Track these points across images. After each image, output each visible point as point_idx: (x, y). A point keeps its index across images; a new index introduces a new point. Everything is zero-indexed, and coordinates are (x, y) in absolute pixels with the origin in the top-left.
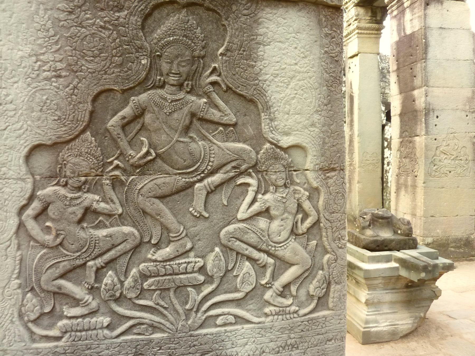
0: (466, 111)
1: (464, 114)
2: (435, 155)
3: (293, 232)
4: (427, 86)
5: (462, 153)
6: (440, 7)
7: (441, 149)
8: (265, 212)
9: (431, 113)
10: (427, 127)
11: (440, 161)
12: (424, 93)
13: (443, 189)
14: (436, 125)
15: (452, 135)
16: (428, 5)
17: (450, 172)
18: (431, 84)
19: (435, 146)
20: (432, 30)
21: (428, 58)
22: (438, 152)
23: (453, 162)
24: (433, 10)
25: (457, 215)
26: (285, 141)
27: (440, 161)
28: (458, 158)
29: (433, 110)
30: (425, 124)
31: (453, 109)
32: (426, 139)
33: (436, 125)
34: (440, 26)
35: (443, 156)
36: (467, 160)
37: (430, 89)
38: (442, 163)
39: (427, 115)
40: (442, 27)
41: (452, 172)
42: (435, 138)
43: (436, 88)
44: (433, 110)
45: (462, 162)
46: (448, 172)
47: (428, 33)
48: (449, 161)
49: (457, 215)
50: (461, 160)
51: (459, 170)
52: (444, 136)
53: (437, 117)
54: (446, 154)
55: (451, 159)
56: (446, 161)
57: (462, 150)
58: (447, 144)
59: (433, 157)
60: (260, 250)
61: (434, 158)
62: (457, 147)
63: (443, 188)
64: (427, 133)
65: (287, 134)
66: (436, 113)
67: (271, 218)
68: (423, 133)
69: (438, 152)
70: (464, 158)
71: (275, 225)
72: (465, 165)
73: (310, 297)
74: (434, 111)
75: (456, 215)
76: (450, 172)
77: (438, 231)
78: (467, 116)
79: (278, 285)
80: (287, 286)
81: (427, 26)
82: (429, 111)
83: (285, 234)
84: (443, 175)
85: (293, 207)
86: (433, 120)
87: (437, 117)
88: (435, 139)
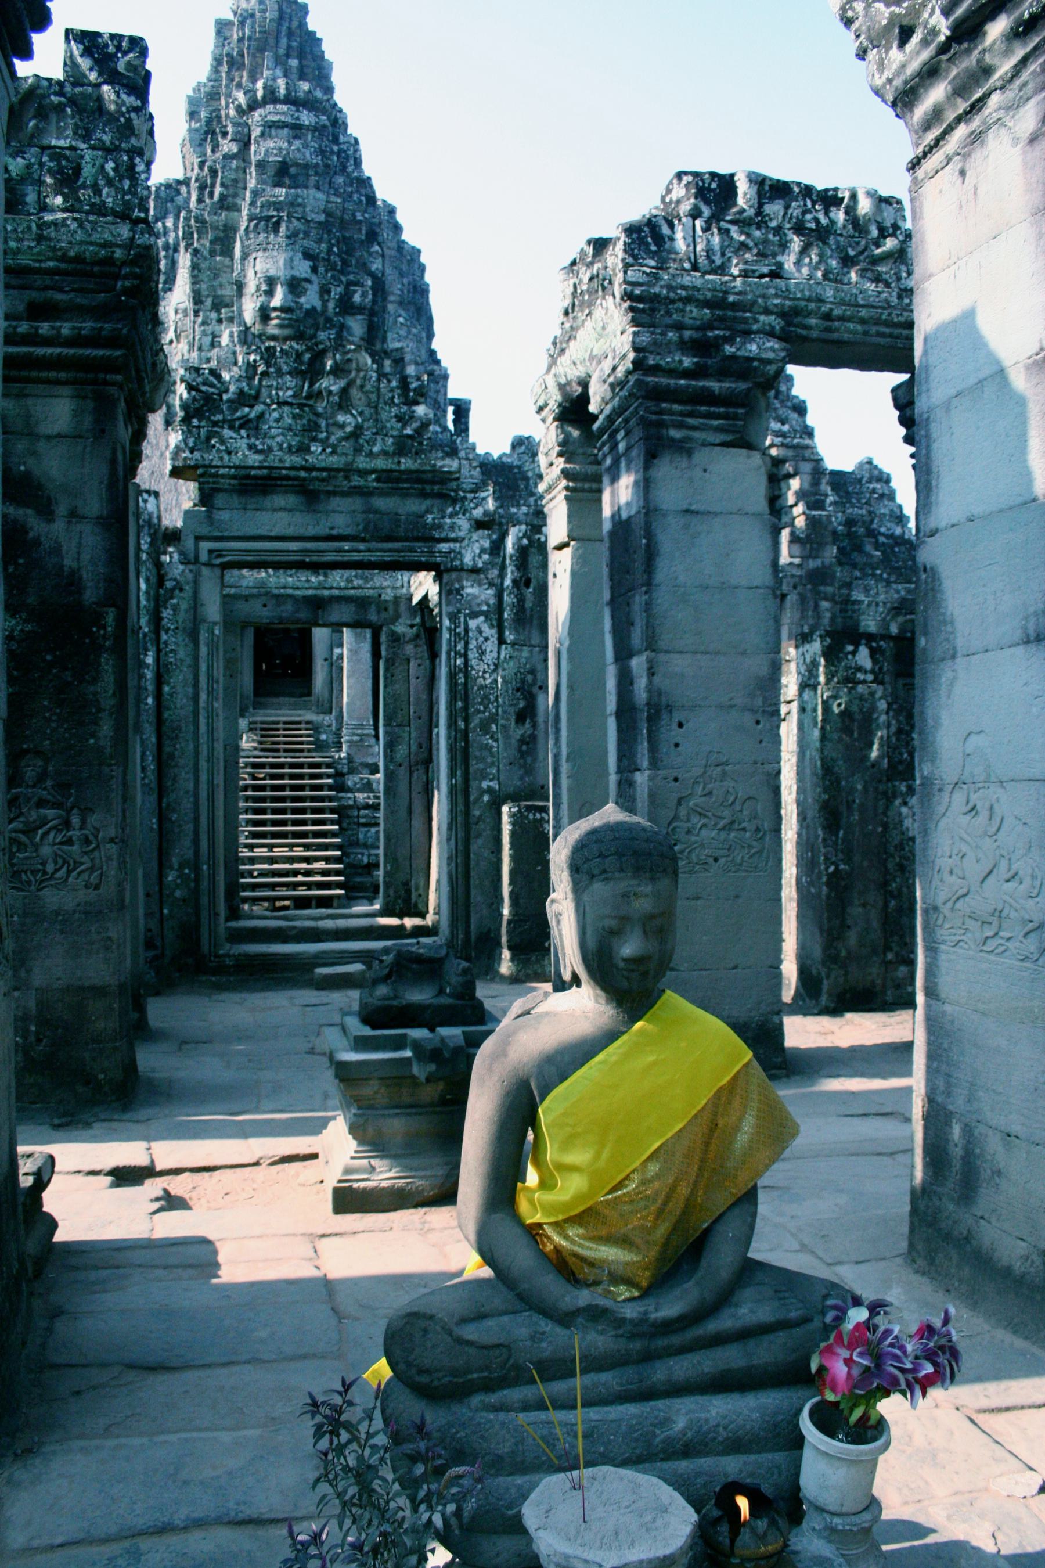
0: (753, 711)
1: (748, 719)
2: (676, 818)
4: (653, 651)
5: (745, 813)
6: (684, 464)
7: (691, 804)
9: (665, 716)
10: (653, 749)
11: (688, 832)
12: (645, 666)
13: (699, 902)
14: (677, 745)
15: (719, 769)
16: (654, 457)
17: (716, 860)
18: (662, 644)
19: (674, 797)
20: (665, 515)
21: (656, 582)
22: (683, 812)
23: (723, 835)
24: (665, 469)
25: (735, 967)
27: (688, 832)
28: (736, 826)
29: (670, 709)
30: (649, 742)
31: (721, 707)
32: (651, 778)
33: (677, 745)
34: (685, 507)
35: (695, 819)
36: (757, 830)
37: (662, 657)
38: (693, 839)
39: (653, 718)
40: (693, 508)
41: (722, 861)
42: (675, 774)
43: (677, 656)
44: (670, 709)
45: (748, 834)
46: (711, 860)
47: (654, 524)
48: (714, 833)
49: (735, 967)
51: (739, 855)
52: (697, 771)
53: (680, 725)
54: (705, 816)
55: (720, 826)
56: (704, 832)
57: (746, 806)
58: (706, 791)
59: (670, 824)
61: (674, 824)
62: (731, 799)
63: (698, 898)
64: (654, 764)
66: (677, 716)
68: (645, 763)
69: (683, 812)
70: (750, 826)
72: (755, 843)
74: (671, 711)
75: (732, 965)
76: (716, 860)
78: (758, 722)
81: (652, 506)
82: (658, 712)
84: (697, 868)
86: (669, 733)
87: (680, 725)
88: (676, 780)
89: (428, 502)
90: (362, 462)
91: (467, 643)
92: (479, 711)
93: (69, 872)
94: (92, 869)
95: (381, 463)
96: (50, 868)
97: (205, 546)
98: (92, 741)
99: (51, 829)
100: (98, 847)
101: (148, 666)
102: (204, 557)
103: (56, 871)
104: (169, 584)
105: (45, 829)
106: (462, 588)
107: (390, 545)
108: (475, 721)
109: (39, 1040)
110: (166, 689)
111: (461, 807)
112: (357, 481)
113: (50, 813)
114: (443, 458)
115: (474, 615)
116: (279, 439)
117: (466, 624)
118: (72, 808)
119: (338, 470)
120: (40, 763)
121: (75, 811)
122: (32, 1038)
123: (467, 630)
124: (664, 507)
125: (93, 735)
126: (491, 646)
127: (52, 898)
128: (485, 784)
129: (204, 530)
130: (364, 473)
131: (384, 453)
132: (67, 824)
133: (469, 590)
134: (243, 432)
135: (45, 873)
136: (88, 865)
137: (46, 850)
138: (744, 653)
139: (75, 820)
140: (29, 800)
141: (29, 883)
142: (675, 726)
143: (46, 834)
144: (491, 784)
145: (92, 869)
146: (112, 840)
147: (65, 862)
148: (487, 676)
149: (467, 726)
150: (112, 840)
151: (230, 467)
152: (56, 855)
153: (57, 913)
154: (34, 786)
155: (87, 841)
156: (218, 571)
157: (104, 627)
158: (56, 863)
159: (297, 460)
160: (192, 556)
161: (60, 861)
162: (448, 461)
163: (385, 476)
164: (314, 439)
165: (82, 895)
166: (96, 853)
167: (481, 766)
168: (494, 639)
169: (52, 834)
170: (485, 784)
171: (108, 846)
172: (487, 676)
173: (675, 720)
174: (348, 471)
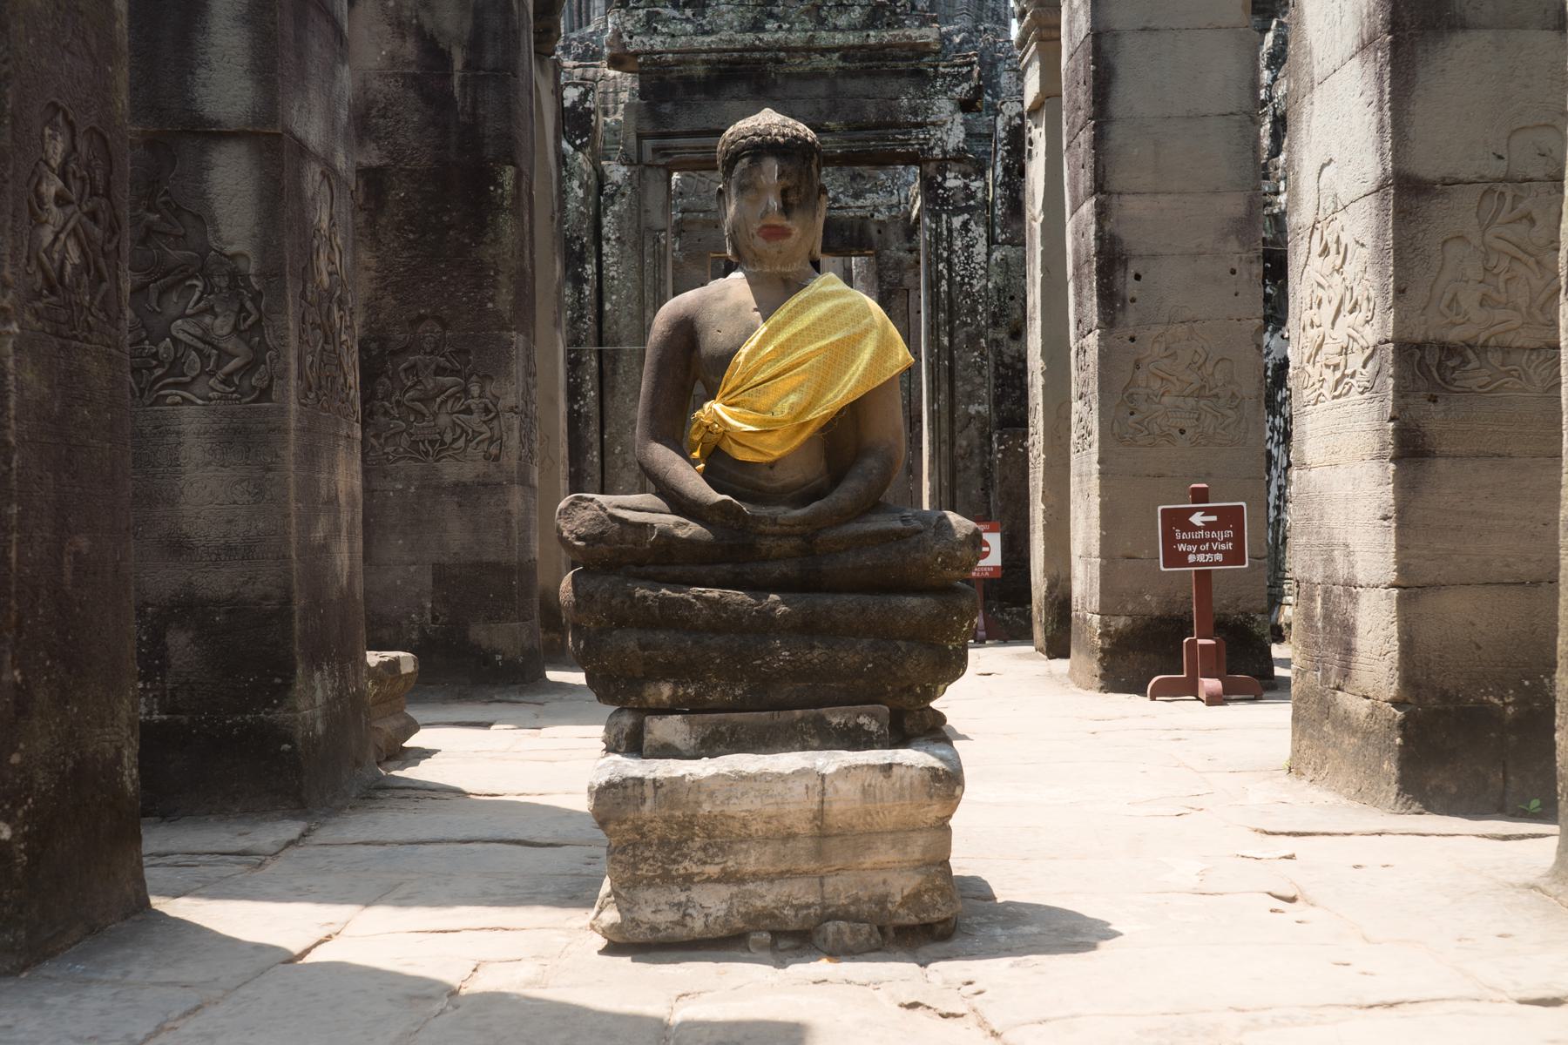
3: (235, 328)
8: (210, 310)
17: (1182, 432)
23: (1191, 402)
26: (230, 250)
34: (1141, 25)
40: (1151, 25)
50: (1216, 396)
53: (1138, 277)
60: (205, 342)
65: (232, 244)
67: (216, 316)
71: (218, 322)
72: (1230, 412)
73: (254, 388)
76: (1182, 432)
77: (1148, 597)
79: (220, 375)
80: (231, 374)
83: (227, 330)
85: (236, 307)
87: (1138, 277)
89: (903, 81)
90: (824, 38)
91: (951, 244)
92: (965, 324)
93: (468, 441)
94: (491, 441)
95: (839, 38)
96: (448, 438)
97: (648, 144)
98: (490, 305)
99: (449, 397)
100: (497, 416)
101: (586, 281)
102: (648, 156)
103: (455, 440)
104: (608, 189)
105: (443, 397)
106: (945, 179)
107: (860, 135)
108: (961, 335)
109: (435, 619)
110: (608, 307)
111: (945, 436)
112: (819, 61)
113: (448, 380)
114: (919, 27)
115: (958, 211)
116: (729, 17)
117: (949, 223)
118: (471, 375)
119: (796, 50)
120: (438, 329)
121: (474, 378)
122: (429, 617)
123: (950, 230)
124: (1117, 27)
125: (492, 299)
126: (981, 248)
127: (450, 471)
128: (973, 409)
129: (647, 127)
130: (825, 51)
131: (852, 28)
132: (466, 392)
133: (951, 183)
134: (689, 12)
135: (443, 443)
136: (488, 434)
137: (444, 420)
138: (1216, 192)
139: (475, 390)
140: (427, 366)
141: (427, 453)
142: (1130, 278)
143: (444, 402)
144: (980, 408)
145: (491, 441)
146: (511, 410)
147: (463, 431)
148: (974, 282)
149: (951, 342)
150: (511, 410)
151: (674, 53)
152: (454, 423)
153: (456, 485)
154: (432, 353)
155: (487, 410)
156: (663, 172)
157: (501, 186)
158: (454, 431)
159: (749, 38)
160: (634, 158)
161: (459, 431)
162: (925, 30)
163: (846, 52)
164: (771, 15)
165: (481, 467)
166: (495, 422)
167: (969, 388)
168: (983, 241)
169: (450, 404)
170: (973, 409)
171: (508, 415)
172: (974, 282)
173: (1132, 271)
174: (809, 49)
